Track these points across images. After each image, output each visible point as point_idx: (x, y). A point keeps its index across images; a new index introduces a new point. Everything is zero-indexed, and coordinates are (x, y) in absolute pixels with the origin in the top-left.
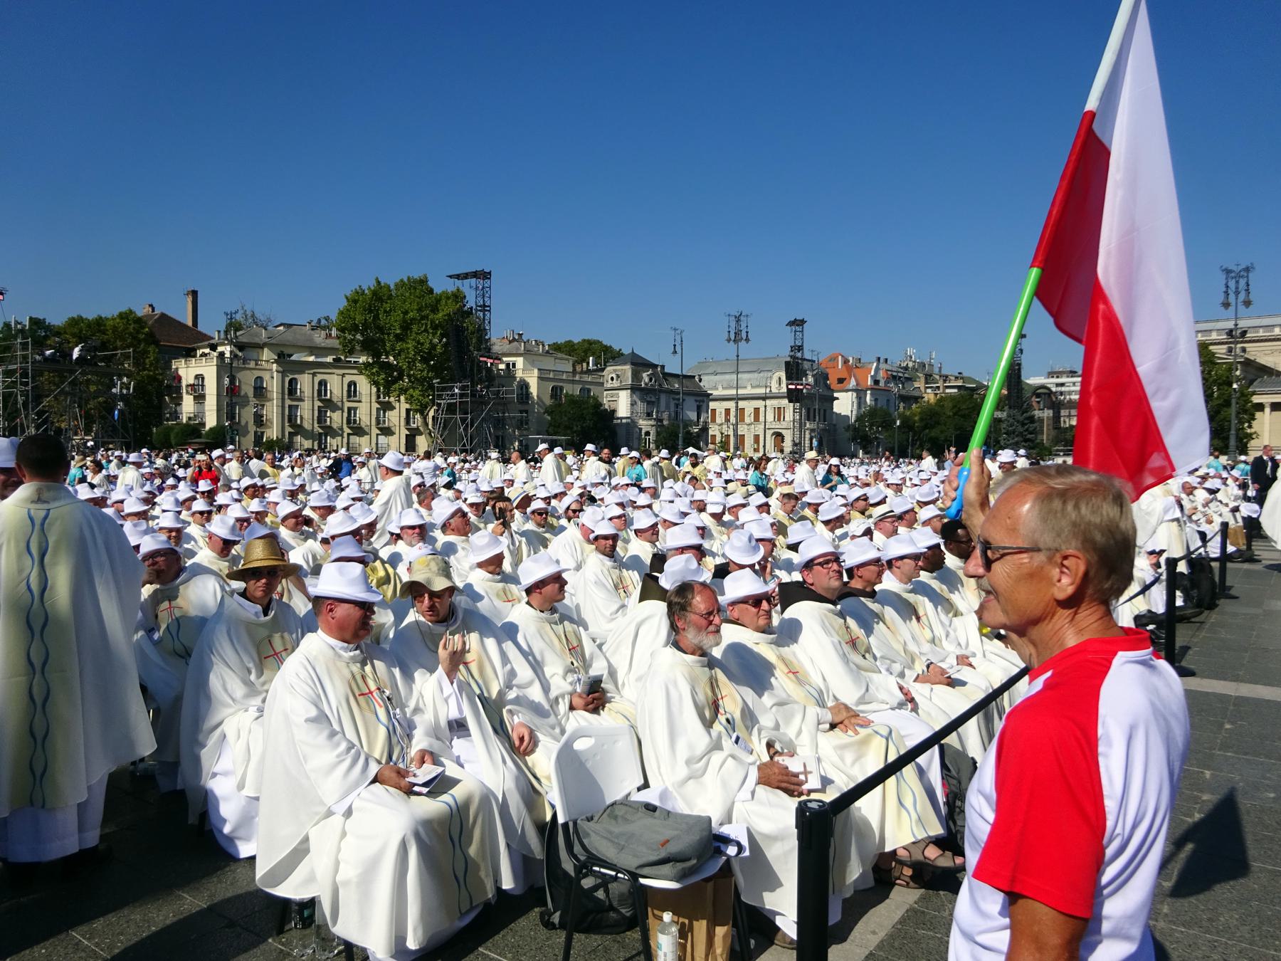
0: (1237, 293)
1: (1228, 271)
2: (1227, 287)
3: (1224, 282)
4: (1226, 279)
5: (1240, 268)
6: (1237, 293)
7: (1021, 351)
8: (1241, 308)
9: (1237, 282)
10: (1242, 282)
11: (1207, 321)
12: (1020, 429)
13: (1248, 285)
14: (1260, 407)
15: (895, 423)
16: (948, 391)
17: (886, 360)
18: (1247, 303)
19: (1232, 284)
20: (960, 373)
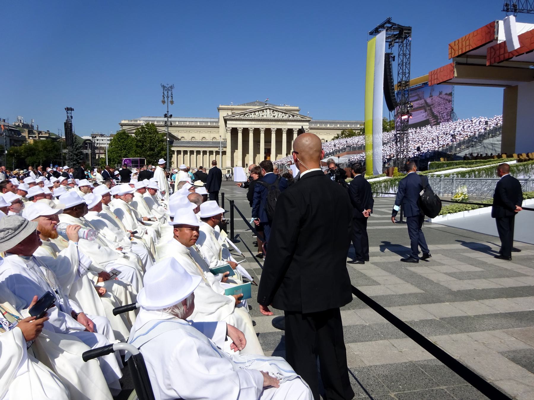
0: (168, 97)
1: (164, 87)
2: (164, 94)
3: (163, 91)
4: (164, 90)
5: (169, 86)
6: (168, 97)
7: (72, 117)
8: (170, 104)
9: (168, 92)
10: (170, 93)
11: (153, 117)
12: (75, 157)
13: (172, 94)
14: (173, 151)
15: (4, 152)
16: (41, 139)
17: (4, 121)
18: (172, 102)
19: (166, 93)
20: (48, 131)
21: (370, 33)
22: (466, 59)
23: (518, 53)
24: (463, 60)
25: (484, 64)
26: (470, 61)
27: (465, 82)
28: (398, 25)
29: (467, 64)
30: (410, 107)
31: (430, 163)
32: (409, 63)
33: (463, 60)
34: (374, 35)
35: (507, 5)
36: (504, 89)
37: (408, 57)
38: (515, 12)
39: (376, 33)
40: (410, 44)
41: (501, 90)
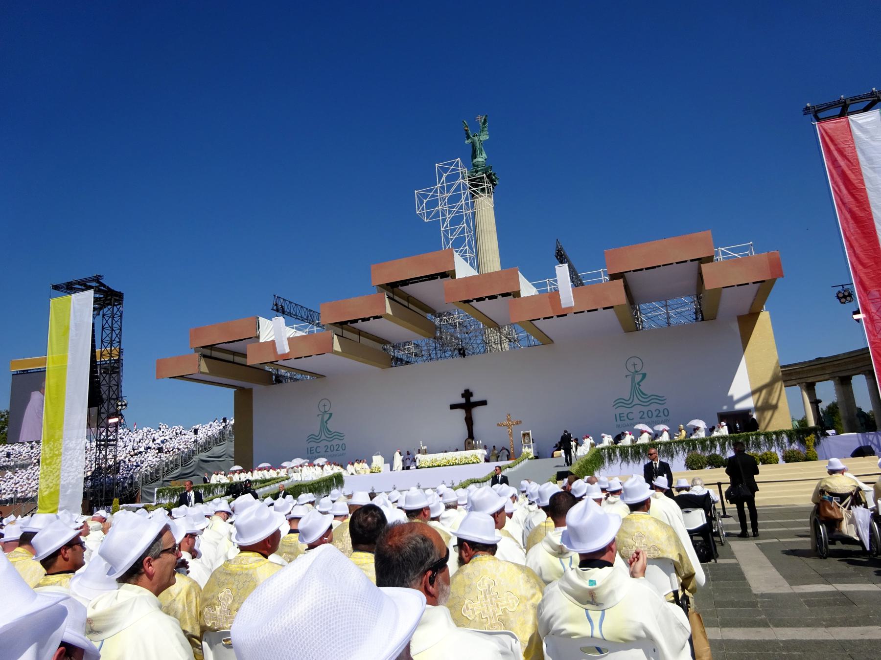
21: (53, 286)
22: (232, 356)
23: (286, 357)
24: (207, 352)
25: (245, 364)
26: (215, 354)
27: (220, 382)
28: (108, 287)
29: (233, 362)
30: (122, 405)
31: (158, 490)
32: (120, 342)
33: (207, 352)
34: (62, 291)
35: (276, 305)
36: (235, 391)
37: (117, 332)
38: (283, 312)
39: (67, 289)
40: (121, 316)
41: (232, 391)
